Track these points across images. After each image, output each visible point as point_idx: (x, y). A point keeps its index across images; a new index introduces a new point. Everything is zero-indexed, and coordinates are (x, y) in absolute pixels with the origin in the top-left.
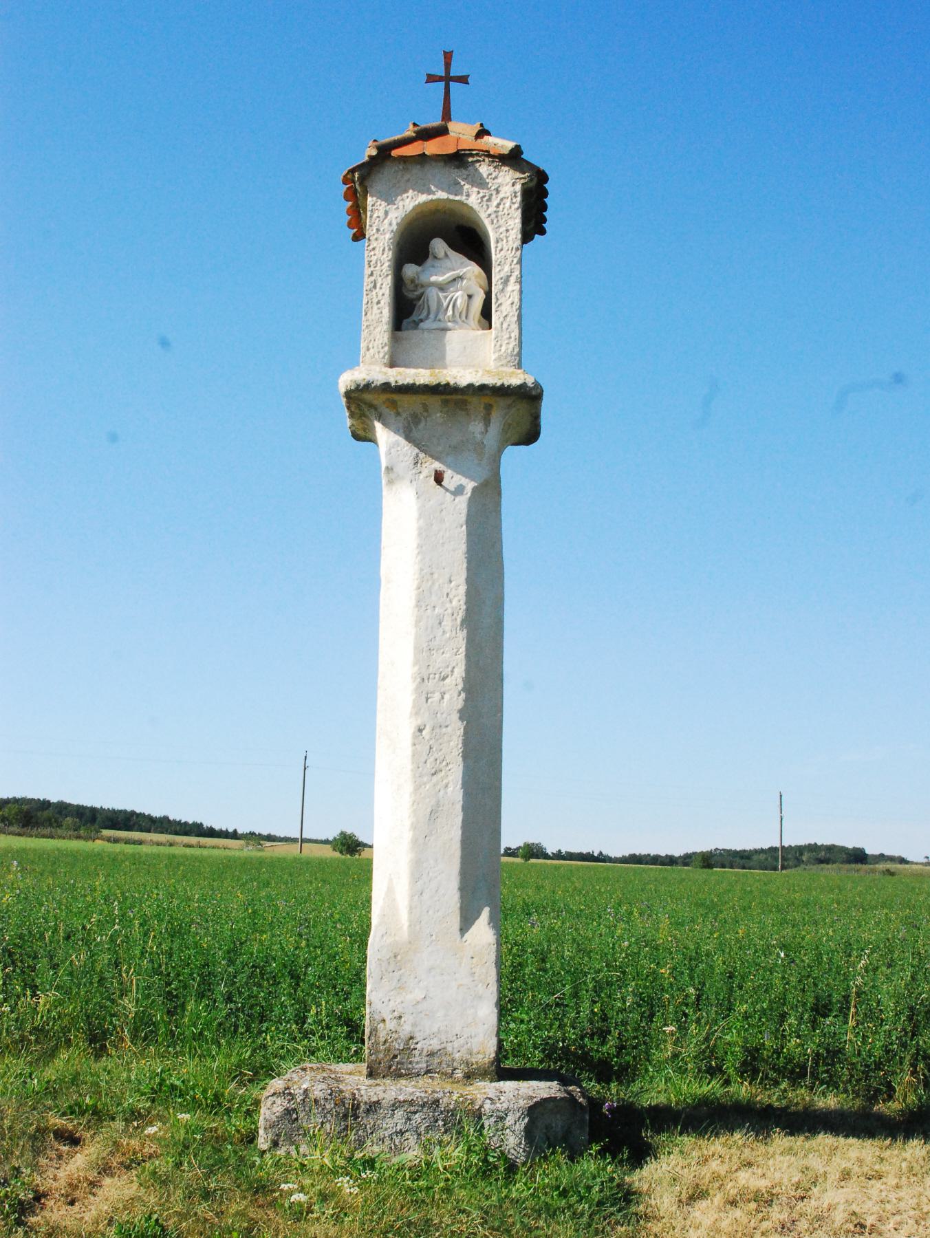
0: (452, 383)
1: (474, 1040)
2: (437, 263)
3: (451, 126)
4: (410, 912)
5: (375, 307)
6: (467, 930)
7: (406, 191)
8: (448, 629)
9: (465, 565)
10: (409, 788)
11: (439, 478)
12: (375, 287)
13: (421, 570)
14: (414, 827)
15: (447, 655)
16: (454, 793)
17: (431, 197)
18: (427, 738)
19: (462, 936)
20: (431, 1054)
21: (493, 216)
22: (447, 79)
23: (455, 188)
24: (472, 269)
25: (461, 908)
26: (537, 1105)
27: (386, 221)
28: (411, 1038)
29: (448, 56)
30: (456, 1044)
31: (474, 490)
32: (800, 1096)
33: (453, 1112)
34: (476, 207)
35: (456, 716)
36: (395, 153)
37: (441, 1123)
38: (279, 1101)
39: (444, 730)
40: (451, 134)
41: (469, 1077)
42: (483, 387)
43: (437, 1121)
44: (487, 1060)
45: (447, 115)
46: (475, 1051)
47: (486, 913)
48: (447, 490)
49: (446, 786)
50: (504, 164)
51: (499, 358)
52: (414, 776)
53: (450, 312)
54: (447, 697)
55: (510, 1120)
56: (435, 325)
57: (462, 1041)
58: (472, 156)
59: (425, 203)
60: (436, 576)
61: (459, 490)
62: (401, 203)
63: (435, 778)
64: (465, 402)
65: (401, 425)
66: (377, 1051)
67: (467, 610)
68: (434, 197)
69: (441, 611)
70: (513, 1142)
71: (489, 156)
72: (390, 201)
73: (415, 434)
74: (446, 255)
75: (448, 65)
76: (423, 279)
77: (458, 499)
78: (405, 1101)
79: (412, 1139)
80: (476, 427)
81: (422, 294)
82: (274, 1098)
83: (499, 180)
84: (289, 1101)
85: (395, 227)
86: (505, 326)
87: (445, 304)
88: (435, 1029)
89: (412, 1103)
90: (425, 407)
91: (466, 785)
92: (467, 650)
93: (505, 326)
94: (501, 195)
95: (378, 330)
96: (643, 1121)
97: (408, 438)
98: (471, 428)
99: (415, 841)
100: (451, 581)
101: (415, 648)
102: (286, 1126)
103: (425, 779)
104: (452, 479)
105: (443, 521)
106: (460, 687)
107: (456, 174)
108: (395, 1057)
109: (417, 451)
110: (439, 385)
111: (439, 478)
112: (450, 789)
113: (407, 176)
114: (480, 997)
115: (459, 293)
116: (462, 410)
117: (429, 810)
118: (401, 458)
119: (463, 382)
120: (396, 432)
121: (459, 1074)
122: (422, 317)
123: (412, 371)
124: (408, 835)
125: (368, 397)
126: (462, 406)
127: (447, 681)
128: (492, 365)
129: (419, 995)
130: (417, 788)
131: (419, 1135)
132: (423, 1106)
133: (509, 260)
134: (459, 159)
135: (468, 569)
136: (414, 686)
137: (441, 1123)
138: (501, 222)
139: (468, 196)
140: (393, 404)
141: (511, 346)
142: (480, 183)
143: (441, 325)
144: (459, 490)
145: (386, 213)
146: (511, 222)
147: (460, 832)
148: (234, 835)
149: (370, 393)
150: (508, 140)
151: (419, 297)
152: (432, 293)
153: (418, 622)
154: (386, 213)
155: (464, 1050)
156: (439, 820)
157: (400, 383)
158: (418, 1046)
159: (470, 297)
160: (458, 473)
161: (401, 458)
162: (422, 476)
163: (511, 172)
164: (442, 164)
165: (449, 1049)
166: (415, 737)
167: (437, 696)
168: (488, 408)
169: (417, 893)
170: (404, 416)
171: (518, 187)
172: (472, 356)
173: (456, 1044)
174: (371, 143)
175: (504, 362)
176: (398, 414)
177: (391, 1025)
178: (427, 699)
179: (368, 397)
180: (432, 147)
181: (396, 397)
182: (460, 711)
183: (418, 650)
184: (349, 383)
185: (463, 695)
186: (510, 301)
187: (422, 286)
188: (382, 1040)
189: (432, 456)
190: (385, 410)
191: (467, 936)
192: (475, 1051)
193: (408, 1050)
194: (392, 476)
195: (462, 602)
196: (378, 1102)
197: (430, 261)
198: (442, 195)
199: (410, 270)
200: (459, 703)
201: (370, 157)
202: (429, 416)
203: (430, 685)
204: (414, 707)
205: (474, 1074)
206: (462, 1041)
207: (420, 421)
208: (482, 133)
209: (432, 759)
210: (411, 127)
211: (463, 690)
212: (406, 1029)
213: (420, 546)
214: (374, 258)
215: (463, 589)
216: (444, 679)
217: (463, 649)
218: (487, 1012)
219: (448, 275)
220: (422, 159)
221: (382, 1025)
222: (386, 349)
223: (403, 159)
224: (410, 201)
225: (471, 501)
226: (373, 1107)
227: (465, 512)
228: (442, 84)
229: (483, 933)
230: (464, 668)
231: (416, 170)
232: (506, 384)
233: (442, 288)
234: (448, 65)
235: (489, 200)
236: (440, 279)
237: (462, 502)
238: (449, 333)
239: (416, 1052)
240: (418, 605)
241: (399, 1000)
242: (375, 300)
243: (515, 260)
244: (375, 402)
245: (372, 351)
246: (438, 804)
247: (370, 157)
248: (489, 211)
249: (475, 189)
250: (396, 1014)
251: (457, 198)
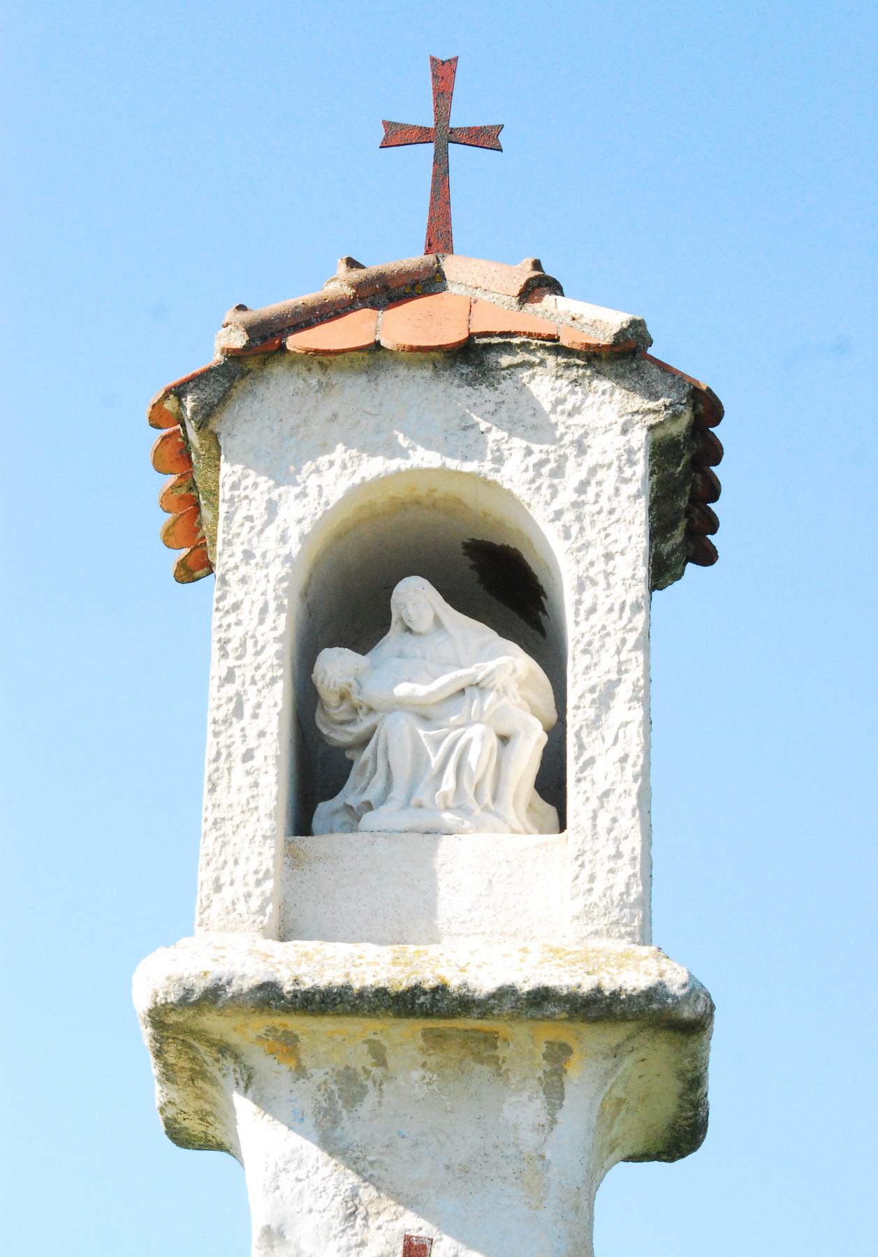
0: (454, 983)
3: (451, 266)
5: (239, 767)
7: (327, 448)
12: (238, 712)
21: (569, 517)
22: (442, 136)
23: (463, 437)
24: (512, 663)
27: (272, 532)
29: (444, 74)
34: (520, 490)
36: (295, 342)
40: (452, 288)
42: (541, 998)
45: (440, 237)
51: (588, 913)
58: (507, 348)
59: (381, 481)
62: (313, 481)
64: (490, 1040)
65: (308, 1106)
71: (559, 350)
72: (282, 474)
73: (352, 1129)
74: (438, 622)
76: (373, 691)
81: (372, 731)
85: (294, 547)
86: (603, 821)
87: (435, 761)
90: (378, 1054)
93: (603, 821)
94: (590, 459)
97: (329, 1143)
109: (353, 1179)
110: (415, 991)
113: (331, 404)
115: (475, 731)
118: (308, 1201)
119: (484, 983)
125: (213, 1023)
133: (612, 643)
134: (470, 357)
138: (590, 534)
139: (499, 460)
140: (288, 1045)
141: (619, 882)
142: (533, 425)
143: (424, 820)
145: (272, 508)
149: (221, 1012)
151: (363, 742)
152: (398, 735)
154: (272, 508)
157: (307, 984)
159: (504, 739)
161: (308, 1201)
163: (619, 394)
168: (558, 1054)
170: (318, 1075)
171: (639, 437)
172: (507, 908)
174: (230, 315)
175: (602, 924)
176: (301, 1072)
179: (213, 1023)
180: (399, 326)
181: (294, 1023)
184: (160, 984)
186: (617, 752)
187: (371, 710)
189: (397, 1197)
190: (261, 1060)
197: (392, 641)
198: (426, 458)
199: (337, 666)
207: (364, 1091)
208: (540, 285)
210: (342, 267)
214: (236, 633)
219: (447, 680)
222: (269, 885)
223: (322, 359)
228: (427, 151)
231: (353, 391)
232: (608, 987)
235: (558, 472)
238: (446, 842)
242: (238, 751)
243: (632, 638)
244: (234, 1039)
245: (227, 892)
248: (557, 505)
249: (519, 443)
251: (469, 467)
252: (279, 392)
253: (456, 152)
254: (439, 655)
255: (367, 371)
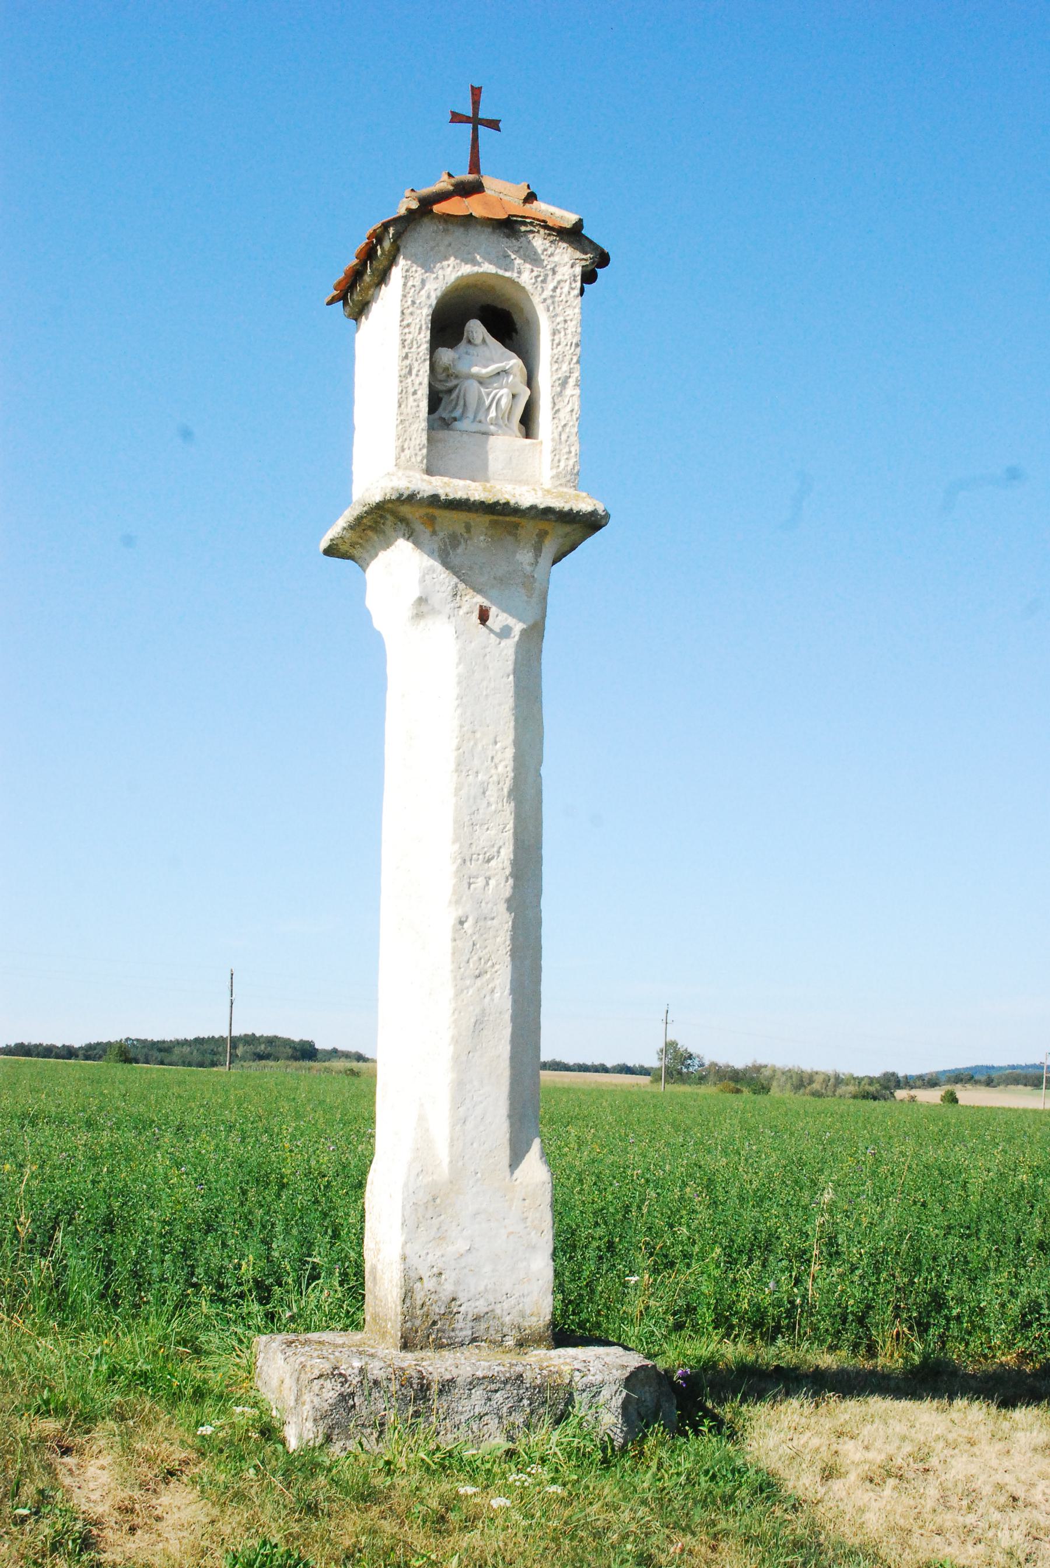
0: (512, 502)
1: (527, 1300)
2: (471, 349)
3: (487, 181)
4: (452, 1145)
5: (411, 398)
6: (518, 1165)
7: (446, 258)
8: (492, 800)
9: (512, 724)
10: (449, 991)
11: (484, 616)
12: (410, 373)
13: (462, 726)
14: (456, 1041)
15: (492, 832)
16: (502, 1000)
17: (476, 269)
18: (470, 932)
19: (512, 1173)
20: (477, 1319)
21: (549, 301)
22: (476, 121)
23: (504, 261)
24: (514, 362)
25: (511, 1140)
26: (633, 1374)
27: (423, 292)
28: (454, 1299)
29: (476, 92)
30: (506, 1305)
31: (523, 632)
32: (779, 1353)
33: (541, 1389)
34: (529, 288)
35: (502, 907)
36: (437, 208)
37: (526, 1402)
38: (328, 1384)
39: (489, 922)
40: (487, 192)
41: (521, 1345)
42: (548, 510)
43: (521, 1400)
44: (542, 1323)
45: (475, 166)
46: (528, 1312)
47: (536, 1145)
48: (491, 630)
49: (493, 991)
50: (562, 240)
51: (557, 476)
52: (455, 978)
53: (493, 413)
54: (492, 882)
55: (606, 1393)
56: (475, 427)
57: (512, 1301)
58: (525, 224)
59: (469, 276)
60: (478, 735)
61: (505, 633)
62: (440, 272)
63: (479, 982)
64: (516, 526)
65: (436, 547)
66: (414, 1317)
67: (515, 778)
68: (481, 270)
69: (485, 778)
70: (610, 1420)
71: (546, 227)
72: (428, 269)
73: (455, 560)
74: (484, 341)
75: (476, 104)
76: (462, 368)
77: (505, 643)
78: (484, 1378)
79: (493, 1423)
80: (524, 557)
81: (456, 386)
82: (321, 1381)
83: (556, 258)
84: (343, 1384)
85: (433, 302)
86: (564, 437)
87: (487, 403)
88: (481, 1288)
89: (492, 1379)
90: (468, 528)
91: (514, 991)
92: (515, 828)
93: (564, 437)
94: (558, 277)
95: (415, 426)
96: (703, 1388)
97: (446, 564)
98: (519, 557)
99: (456, 1059)
100: (496, 743)
101: (456, 822)
102: (340, 1415)
103: (468, 982)
104: (498, 618)
105: (486, 668)
106: (508, 871)
107: (506, 244)
108: (434, 1323)
109: (456, 580)
110: (497, 503)
111: (484, 616)
112: (497, 995)
113: (448, 239)
114: (534, 1247)
115: (505, 391)
116: (510, 533)
117: (473, 1020)
118: (437, 588)
119: (526, 502)
120: (431, 554)
121: (510, 1342)
122: (457, 413)
123: (461, 483)
124: (448, 1051)
125: (405, 510)
126: (513, 530)
127: (493, 863)
128: (548, 484)
129: (462, 1246)
130: (459, 993)
131: (500, 1418)
132: (505, 1382)
133: (568, 357)
134: (509, 226)
135: (516, 729)
136: (454, 868)
137: (526, 1402)
138: (559, 310)
139: (519, 273)
140: (431, 520)
141: (571, 462)
142: (534, 259)
143: (483, 428)
144: (505, 633)
145: (423, 282)
146: (569, 311)
147: (509, 1048)
148: (603, 1069)
149: (412, 505)
150: (571, 211)
151: (450, 391)
152: (472, 388)
153: (458, 790)
154: (423, 282)
155: (514, 1312)
156: (485, 1032)
157: (451, 497)
158: (462, 1309)
159: (514, 396)
160: (504, 611)
161: (437, 588)
162: (461, 612)
163: (570, 250)
164: (490, 230)
165: (498, 1312)
166: (455, 931)
167: (481, 882)
168: (542, 535)
169: (460, 1121)
170: (441, 535)
171: (578, 270)
172: (528, 473)
173: (506, 1305)
174: (408, 193)
175: (563, 481)
176: (434, 533)
177: (429, 1284)
178: (470, 884)
179: (405, 510)
180: (473, 206)
181: (437, 512)
182: (509, 901)
183: (458, 824)
184: (388, 491)
185: (511, 881)
186: (569, 408)
187: (457, 377)
188: (419, 1303)
189: (474, 589)
190: (419, 527)
191: (517, 1172)
192: (528, 1312)
193: (450, 1314)
194: (424, 608)
195: (510, 768)
196: (452, 1381)
197: (463, 346)
198: (488, 268)
199: (446, 355)
200: (507, 890)
201: (409, 210)
202: (470, 538)
203: (473, 867)
204: (455, 892)
205: (527, 1340)
206: (512, 1301)
207: (459, 543)
208: (531, 197)
209: (475, 958)
210: (446, 177)
211: (511, 874)
212: (448, 1288)
213: (460, 697)
214: (409, 337)
215: (510, 752)
216: (489, 861)
217: (510, 826)
218: (541, 1267)
219: (492, 368)
220: (468, 220)
221: (418, 1284)
222: (425, 451)
223: (448, 219)
224: (452, 272)
225: (519, 645)
226: (447, 1386)
227: (512, 658)
228: (481, 129)
229: (534, 1169)
230: (511, 848)
231: (458, 233)
232: (575, 509)
233: (482, 381)
234: (476, 104)
235: (544, 281)
236: (484, 371)
237: (509, 647)
238: (492, 439)
239: (459, 1317)
240: (458, 770)
241: (439, 1254)
242: (411, 390)
243: (575, 360)
244: (409, 516)
245: (407, 452)
246: (483, 1010)
247: (409, 210)
248: (544, 296)
249: (528, 266)
250: (435, 1270)
251: (508, 274)
252: (427, 229)
253: (481, 129)
254: (484, 357)
255: (494, 228)
